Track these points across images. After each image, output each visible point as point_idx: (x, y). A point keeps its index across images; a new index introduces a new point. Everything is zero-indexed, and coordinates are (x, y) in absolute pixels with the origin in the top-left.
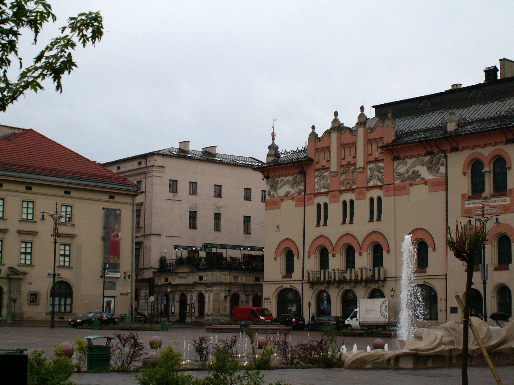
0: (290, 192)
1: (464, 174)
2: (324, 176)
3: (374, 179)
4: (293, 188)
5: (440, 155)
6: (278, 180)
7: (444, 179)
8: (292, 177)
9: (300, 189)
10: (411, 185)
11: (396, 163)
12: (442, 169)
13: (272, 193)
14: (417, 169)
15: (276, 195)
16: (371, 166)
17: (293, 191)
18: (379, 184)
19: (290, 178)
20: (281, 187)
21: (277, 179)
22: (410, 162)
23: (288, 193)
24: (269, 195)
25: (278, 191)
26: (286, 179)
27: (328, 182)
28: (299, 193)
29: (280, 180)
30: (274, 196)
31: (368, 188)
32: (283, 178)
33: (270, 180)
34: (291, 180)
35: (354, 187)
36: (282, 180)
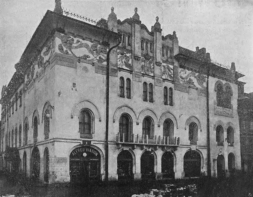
0: (90, 57)
1: (215, 91)
2: (126, 56)
3: (166, 74)
4: (92, 53)
5: (203, 75)
6: (73, 40)
7: (206, 90)
8: (92, 44)
9: (100, 58)
10: (189, 87)
11: (180, 69)
12: (205, 85)
13: (65, 49)
14: (192, 78)
15: (70, 52)
16: (165, 64)
17: (92, 57)
18: (169, 79)
19: (90, 44)
20: (76, 47)
21: (72, 37)
22: (188, 72)
23: (86, 57)
24: (61, 49)
25: (73, 50)
26: (83, 42)
27: (130, 62)
28: (100, 60)
29: (76, 40)
30: (67, 53)
31: (164, 80)
32: (81, 40)
33: (63, 35)
34: (90, 46)
35: (152, 75)
36: (78, 41)
